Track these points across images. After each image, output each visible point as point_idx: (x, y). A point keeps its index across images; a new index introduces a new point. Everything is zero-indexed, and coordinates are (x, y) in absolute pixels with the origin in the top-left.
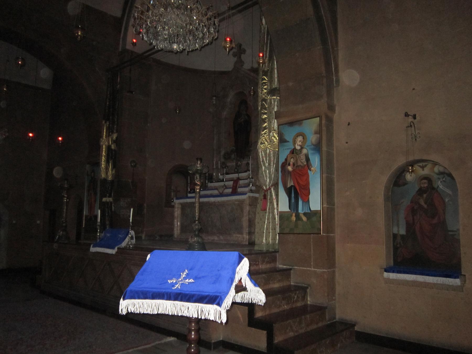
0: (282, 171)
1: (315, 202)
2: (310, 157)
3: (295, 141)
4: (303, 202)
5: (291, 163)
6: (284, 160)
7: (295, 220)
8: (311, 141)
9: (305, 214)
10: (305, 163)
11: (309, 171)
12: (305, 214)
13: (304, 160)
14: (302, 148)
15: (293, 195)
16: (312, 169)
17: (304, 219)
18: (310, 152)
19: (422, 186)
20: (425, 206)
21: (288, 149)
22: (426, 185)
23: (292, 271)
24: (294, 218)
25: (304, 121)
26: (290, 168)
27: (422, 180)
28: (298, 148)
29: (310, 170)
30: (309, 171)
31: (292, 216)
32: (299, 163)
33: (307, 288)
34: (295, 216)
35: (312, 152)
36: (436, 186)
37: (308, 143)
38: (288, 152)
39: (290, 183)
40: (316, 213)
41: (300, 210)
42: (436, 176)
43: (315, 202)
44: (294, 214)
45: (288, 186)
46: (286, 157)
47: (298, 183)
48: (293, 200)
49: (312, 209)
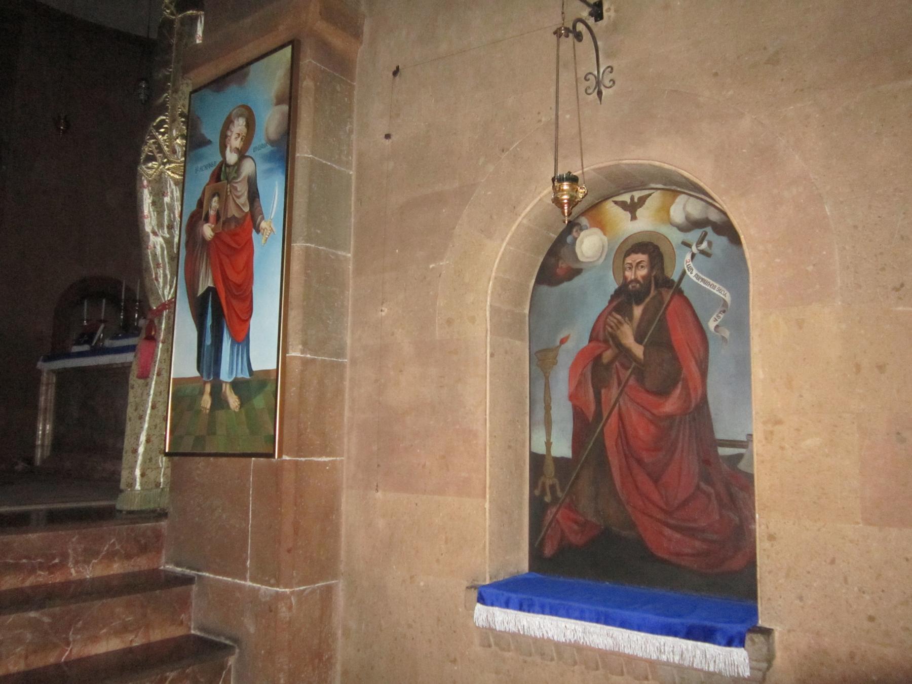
3: (226, 136)
5: (212, 213)
6: (194, 207)
7: (208, 406)
8: (267, 134)
9: (236, 385)
10: (246, 209)
13: (243, 200)
15: (209, 322)
16: (263, 225)
17: (233, 401)
19: (630, 275)
20: (638, 350)
21: (206, 168)
22: (643, 272)
23: (195, 588)
24: (206, 401)
25: (253, 67)
27: (628, 254)
29: (258, 231)
30: (254, 232)
31: (202, 393)
32: (233, 211)
33: (225, 649)
34: (211, 394)
35: (267, 166)
36: (675, 277)
37: (259, 139)
38: (206, 175)
42: (675, 237)
44: (208, 388)
46: (199, 196)
47: (225, 278)
48: (208, 341)
49: (255, 368)
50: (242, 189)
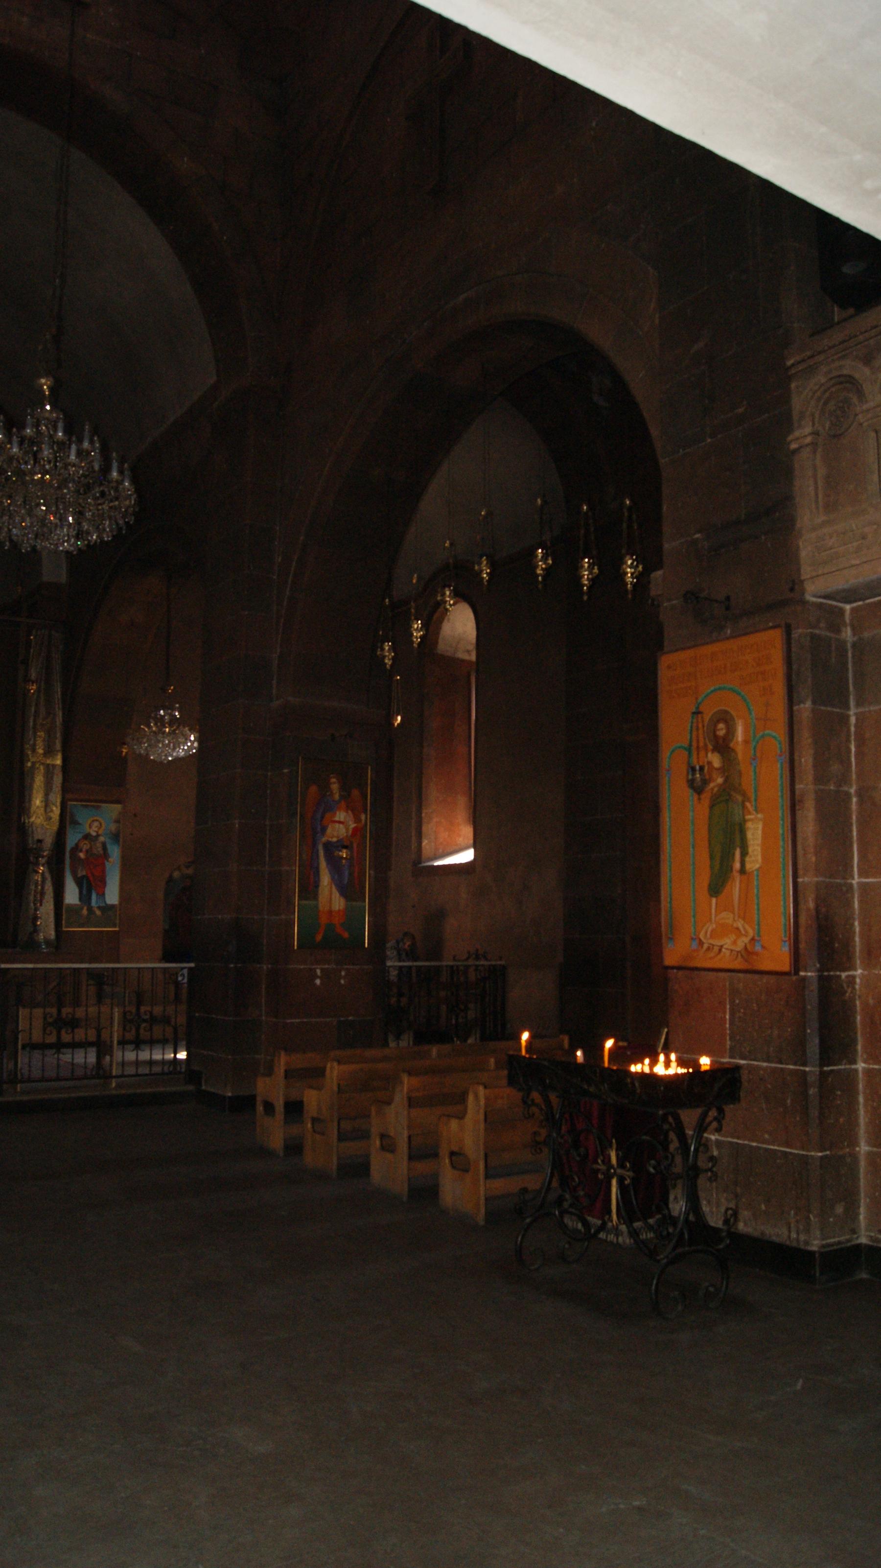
0: (70, 858)
1: (112, 896)
2: (109, 846)
4: (98, 894)
9: (99, 908)
10: (102, 852)
11: (107, 863)
12: (99, 908)
13: (100, 850)
14: (98, 836)
17: (98, 913)
18: (108, 841)
24: (85, 912)
25: (104, 805)
26: (82, 855)
28: (94, 834)
31: (82, 909)
32: (95, 851)
34: (88, 910)
38: (80, 836)
39: (81, 873)
40: (113, 907)
41: (94, 903)
43: (112, 896)
44: (85, 908)
45: (79, 875)
48: (84, 892)
50: (99, 845)
